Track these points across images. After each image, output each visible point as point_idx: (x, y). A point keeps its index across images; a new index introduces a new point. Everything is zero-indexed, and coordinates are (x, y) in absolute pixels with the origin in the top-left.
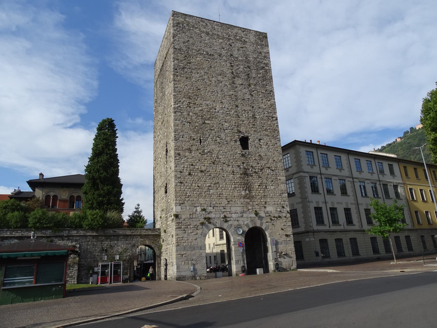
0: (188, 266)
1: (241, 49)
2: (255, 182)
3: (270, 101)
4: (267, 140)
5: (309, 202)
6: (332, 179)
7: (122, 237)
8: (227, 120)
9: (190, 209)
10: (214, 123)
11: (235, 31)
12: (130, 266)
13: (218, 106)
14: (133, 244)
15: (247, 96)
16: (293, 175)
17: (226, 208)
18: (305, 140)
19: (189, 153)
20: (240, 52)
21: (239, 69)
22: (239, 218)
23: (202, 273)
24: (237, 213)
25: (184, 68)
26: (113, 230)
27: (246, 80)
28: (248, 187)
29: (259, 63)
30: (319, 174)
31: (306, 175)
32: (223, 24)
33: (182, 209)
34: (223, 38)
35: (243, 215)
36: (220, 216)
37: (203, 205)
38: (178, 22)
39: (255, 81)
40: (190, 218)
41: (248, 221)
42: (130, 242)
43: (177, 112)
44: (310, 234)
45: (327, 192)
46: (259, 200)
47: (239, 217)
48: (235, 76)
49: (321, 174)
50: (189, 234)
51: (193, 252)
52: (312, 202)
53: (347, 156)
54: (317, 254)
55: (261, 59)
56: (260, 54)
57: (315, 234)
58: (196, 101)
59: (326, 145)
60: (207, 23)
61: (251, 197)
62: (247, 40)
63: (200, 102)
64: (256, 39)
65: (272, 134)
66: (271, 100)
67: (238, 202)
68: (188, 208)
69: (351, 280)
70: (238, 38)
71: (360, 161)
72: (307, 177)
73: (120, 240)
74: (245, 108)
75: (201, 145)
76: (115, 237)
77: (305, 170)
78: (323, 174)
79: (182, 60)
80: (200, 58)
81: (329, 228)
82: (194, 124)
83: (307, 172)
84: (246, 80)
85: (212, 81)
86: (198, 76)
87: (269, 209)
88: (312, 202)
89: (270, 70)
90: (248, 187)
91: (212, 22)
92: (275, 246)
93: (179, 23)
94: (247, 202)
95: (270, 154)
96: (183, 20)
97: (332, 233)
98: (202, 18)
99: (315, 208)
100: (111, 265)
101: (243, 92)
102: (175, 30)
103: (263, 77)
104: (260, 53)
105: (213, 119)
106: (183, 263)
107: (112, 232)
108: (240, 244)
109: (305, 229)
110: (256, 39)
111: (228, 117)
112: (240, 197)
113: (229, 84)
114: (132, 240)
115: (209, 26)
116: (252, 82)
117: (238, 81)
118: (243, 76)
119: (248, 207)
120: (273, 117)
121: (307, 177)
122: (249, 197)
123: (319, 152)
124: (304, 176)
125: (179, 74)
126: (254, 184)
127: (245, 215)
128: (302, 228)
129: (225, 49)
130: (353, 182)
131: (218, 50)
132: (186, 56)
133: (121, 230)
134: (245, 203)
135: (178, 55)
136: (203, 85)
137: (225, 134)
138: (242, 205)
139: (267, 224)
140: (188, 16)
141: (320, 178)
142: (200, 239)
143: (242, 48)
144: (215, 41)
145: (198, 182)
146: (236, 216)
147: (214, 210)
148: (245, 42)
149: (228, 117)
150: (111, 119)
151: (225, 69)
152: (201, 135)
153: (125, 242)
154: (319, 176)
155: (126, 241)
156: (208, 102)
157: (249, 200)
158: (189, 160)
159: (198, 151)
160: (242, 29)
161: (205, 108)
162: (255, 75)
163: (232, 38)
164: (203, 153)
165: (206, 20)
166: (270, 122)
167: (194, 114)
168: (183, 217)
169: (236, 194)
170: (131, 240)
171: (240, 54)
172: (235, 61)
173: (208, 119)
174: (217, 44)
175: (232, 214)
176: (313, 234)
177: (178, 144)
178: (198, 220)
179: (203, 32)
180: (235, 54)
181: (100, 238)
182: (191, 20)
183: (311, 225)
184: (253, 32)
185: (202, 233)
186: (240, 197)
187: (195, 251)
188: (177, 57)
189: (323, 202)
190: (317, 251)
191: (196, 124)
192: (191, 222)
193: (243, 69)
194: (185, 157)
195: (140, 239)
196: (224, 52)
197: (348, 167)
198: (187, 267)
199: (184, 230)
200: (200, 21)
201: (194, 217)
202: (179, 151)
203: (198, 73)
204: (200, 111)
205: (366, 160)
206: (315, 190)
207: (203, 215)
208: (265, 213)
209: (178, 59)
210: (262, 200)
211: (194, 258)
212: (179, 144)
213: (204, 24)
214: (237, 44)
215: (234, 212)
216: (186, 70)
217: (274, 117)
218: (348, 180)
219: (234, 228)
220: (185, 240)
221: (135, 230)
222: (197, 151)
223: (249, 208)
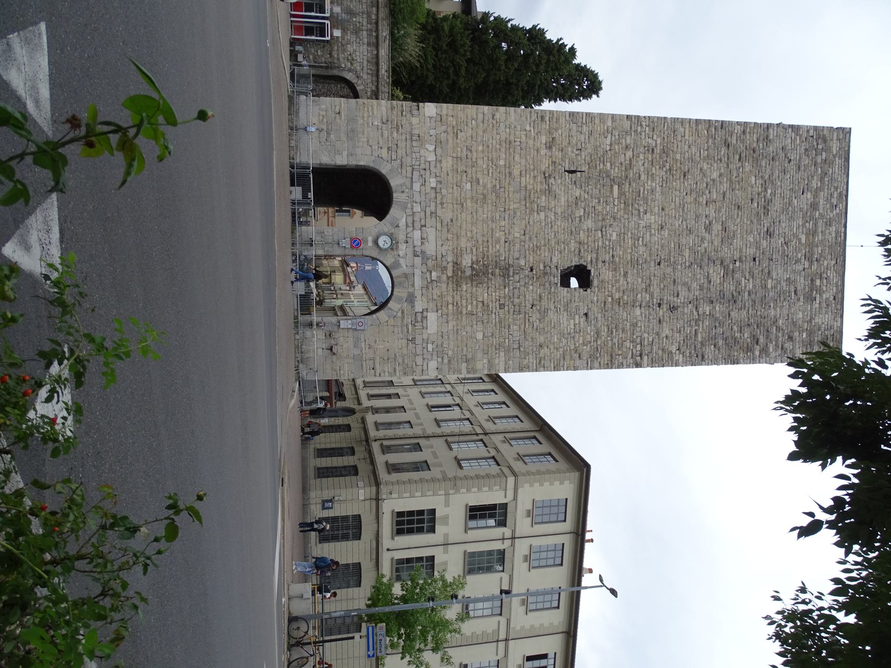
0: (317, 123)
1: (793, 289)
3: (678, 352)
4: (587, 333)
5: (447, 494)
6: (499, 618)
7: (375, 52)
8: (624, 238)
9: (431, 136)
11: (831, 274)
12: (321, 67)
13: (650, 218)
14: (361, 75)
16: (508, 467)
17: (434, 219)
18: (592, 540)
19: (546, 144)
20: (784, 284)
21: (743, 279)
22: (412, 246)
23: (302, 151)
24: (422, 243)
26: (388, 37)
27: (722, 294)
29: (765, 332)
30: (514, 532)
31: (510, 494)
32: (842, 247)
33: (431, 118)
34: (811, 245)
35: (418, 256)
36: (416, 203)
37: (438, 166)
38: (829, 139)
39: (721, 318)
40: (412, 135)
41: (405, 267)
42: (365, 68)
43: (629, 122)
44: (374, 488)
45: (472, 555)
46: (450, 300)
47: (414, 247)
49: (513, 538)
50: (380, 131)
51: (344, 138)
52: (447, 504)
53: (560, 630)
54: (326, 504)
55: (777, 337)
56: (789, 338)
57: (374, 502)
58: (658, 167)
59: (587, 546)
60: (837, 209)
61: (457, 281)
62: (817, 306)
63: (658, 178)
64: (823, 329)
65: (601, 348)
66: (681, 356)
67: (445, 247)
68: (432, 132)
69: (275, 175)
70: (818, 282)
71: (554, 608)
72: (505, 497)
73: (369, 49)
74: (655, 286)
75: (565, 171)
76: (374, 40)
77: (520, 491)
78: (513, 545)
79: (743, 143)
80: (756, 184)
81: (385, 547)
82: (608, 160)
83: (515, 498)
84: (722, 294)
85: (707, 209)
86: (715, 175)
88: (447, 504)
89: (753, 361)
91: (843, 221)
92: (350, 326)
93: (825, 141)
94: (445, 268)
95: (556, 340)
96: (834, 152)
97: (374, 556)
98: (847, 196)
99: (433, 512)
100: (324, 18)
102: (808, 131)
103: (736, 340)
104: (791, 338)
105: (622, 205)
106: (323, 113)
107: (384, 34)
108: (357, 242)
109: (384, 481)
110: (823, 329)
111: (630, 241)
112: (458, 254)
113: (706, 249)
114: (368, 74)
115: (832, 211)
116: (717, 309)
117: (716, 274)
119: (435, 271)
120: (641, 355)
121: (505, 497)
122: (457, 277)
123: (567, 541)
124: (506, 487)
125: (714, 133)
126: (486, 291)
127: (418, 261)
129: (786, 248)
130: (498, 641)
131: (781, 229)
132: (754, 152)
133: (387, 59)
134: (445, 264)
135: (755, 135)
136: (696, 187)
137: (593, 229)
138: (439, 257)
139: (400, 314)
140: (846, 164)
141: (504, 533)
142: (369, 152)
143: (795, 292)
144: (801, 224)
145: (486, 158)
146: (417, 240)
147: (428, 191)
148: (810, 299)
149: (630, 241)
150: (601, 89)
151: (737, 242)
152: (587, 172)
153: (365, 58)
154: (507, 531)
155: (368, 61)
156: (658, 195)
157: (450, 274)
158: (531, 142)
159: (550, 163)
160: (840, 296)
161: (646, 188)
162: (735, 317)
163: (814, 267)
164: (547, 177)
165: (844, 207)
166: (628, 346)
167: (630, 160)
168: (415, 120)
170: (369, 71)
171: (780, 284)
172: (760, 269)
173: (621, 194)
174: (795, 229)
175: (420, 230)
176: (374, 497)
177: (562, 120)
178: (409, 151)
179: (816, 196)
181: (374, 9)
182: (837, 169)
183: (394, 496)
184: (839, 325)
185: (382, 158)
186: (458, 254)
187: (345, 139)
188: (750, 133)
189: (446, 536)
190: (336, 505)
191: (608, 164)
192: (404, 136)
193: (745, 287)
194: (537, 134)
195: (369, 90)
197: (532, 627)
198: (315, 120)
199: (388, 121)
200: (839, 190)
201: (414, 144)
202: (548, 122)
203: (721, 175)
204: (637, 175)
205: (555, 653)
206: (476, 513)
207: (418, 163)
208: (422, 313)
209: (744, 132)
210: (450, 307)
211: (332, 136)
212: (564, 122)
213: (834, 201)
214: (802, 279)
215: (425, 236)
216: (724, 150)
217: (641, 359)
218: (501, 623)
219: (390, 232)
220: (368, 120)
221: (388, 81)
222: (552, 162)
223: (434, 274)
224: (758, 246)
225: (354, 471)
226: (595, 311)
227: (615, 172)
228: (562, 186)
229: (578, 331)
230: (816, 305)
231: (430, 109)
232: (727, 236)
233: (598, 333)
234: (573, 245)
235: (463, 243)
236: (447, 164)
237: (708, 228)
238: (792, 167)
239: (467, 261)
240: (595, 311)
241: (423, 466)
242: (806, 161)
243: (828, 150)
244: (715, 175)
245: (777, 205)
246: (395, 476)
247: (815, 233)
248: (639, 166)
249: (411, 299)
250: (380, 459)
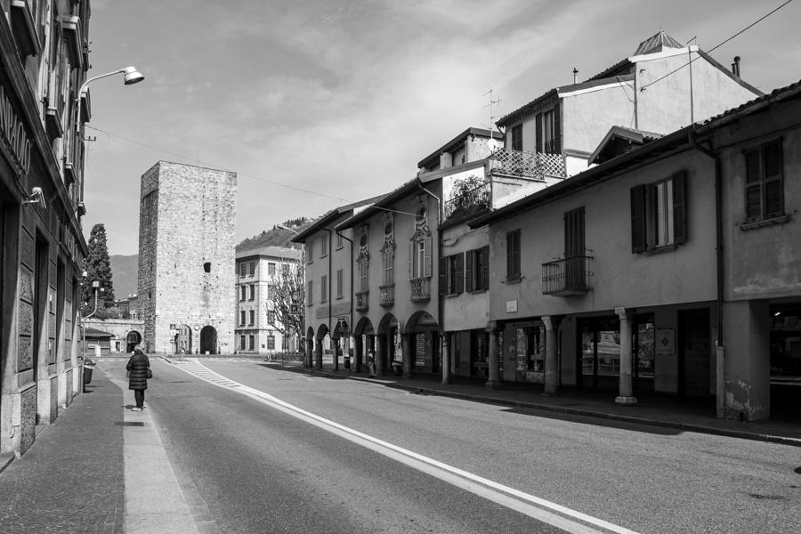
2: (211, 295)
10: (186, 252)
15: (214, 230)
25: (166, 210)
28: (206, 299)
34: (199, 181)
54: (263, 346)
86: (176, 216)
87: (219, 314)
90: (206, 299)
101: (209, 227)
112: (200, 305)
118: (212, 213)
122: (206, 306)
128: (254, 327)
151: (198, 209)
164: (177, 275)
169: (197, 303)
180: (207, 194)
196: (198, 194)
225: (252, 337)
227: (176, 252)
228: (181, 269)
229: (223, 268)
231: (157, 312)
232: (196, 213)
235: (197, 303)
236: (174, 307)
237: (193, 220)
238: (173, 186)
239: (202, 303)
241: (252, 312)
244: (176, 216)
245: (187, 193)
246: (255, 324)
248: (173, 243)
249: (212, 320)
250: (246, 327)
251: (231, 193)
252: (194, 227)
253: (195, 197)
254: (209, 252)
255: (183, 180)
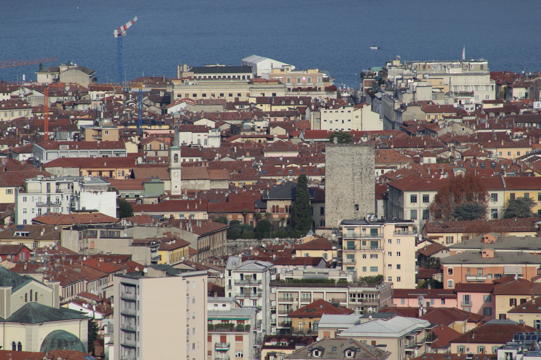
10: (343, 199)
13: (345, 192)
20: (358, 161)
25: (330, 175)
34: (350, 155)
48: (354, 174)
86: (336, 178)
104: (369, 159)
117: (356, 177)
118: (359, 174)
154: (418, 210)
163: (355, 154)
173: (341, 198)
180: (356, 162)
196: (349, 163)
224: (350, 168)
226: (363, 203)
230: (362, 153)
232: (349, 175)
233: (367, 203)
234: (351, 208)
237: (347, 179)
238: (334, 160)
240: (363, 203)
242: (332, 157)
243: (330, 152)
245: (342, 164)
247: (347, 154)
251: (371, 160)
252: (347, 183)
253: (348, 165)
254: (358, 198)
255: (340, 156)
